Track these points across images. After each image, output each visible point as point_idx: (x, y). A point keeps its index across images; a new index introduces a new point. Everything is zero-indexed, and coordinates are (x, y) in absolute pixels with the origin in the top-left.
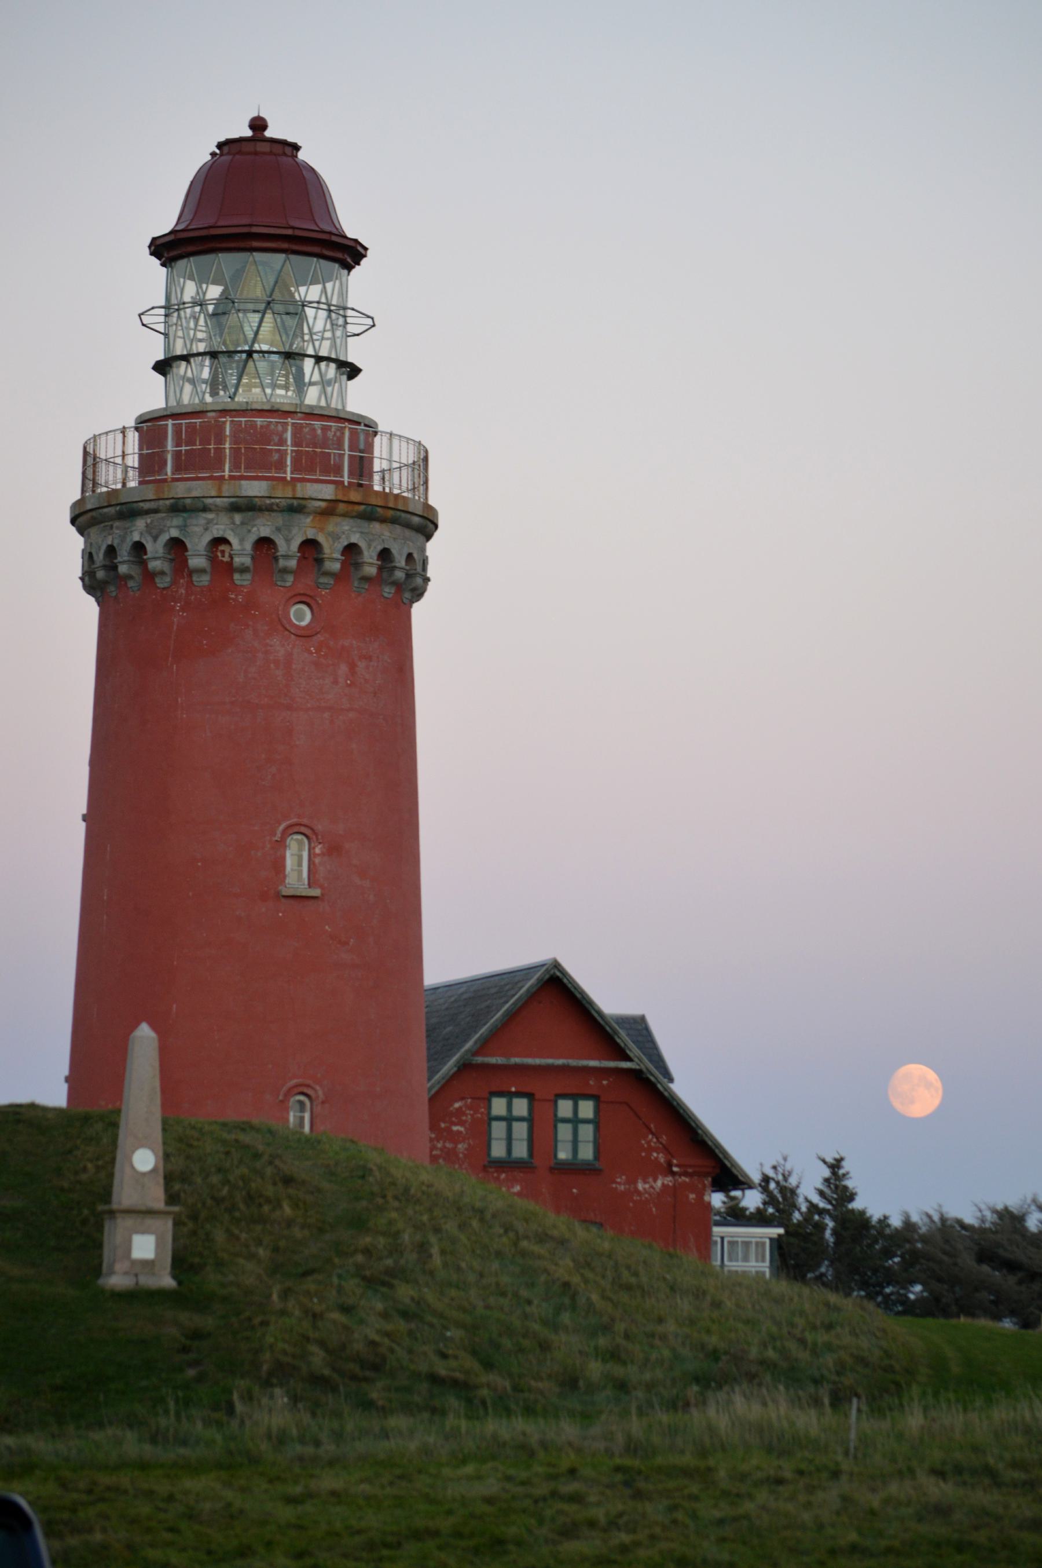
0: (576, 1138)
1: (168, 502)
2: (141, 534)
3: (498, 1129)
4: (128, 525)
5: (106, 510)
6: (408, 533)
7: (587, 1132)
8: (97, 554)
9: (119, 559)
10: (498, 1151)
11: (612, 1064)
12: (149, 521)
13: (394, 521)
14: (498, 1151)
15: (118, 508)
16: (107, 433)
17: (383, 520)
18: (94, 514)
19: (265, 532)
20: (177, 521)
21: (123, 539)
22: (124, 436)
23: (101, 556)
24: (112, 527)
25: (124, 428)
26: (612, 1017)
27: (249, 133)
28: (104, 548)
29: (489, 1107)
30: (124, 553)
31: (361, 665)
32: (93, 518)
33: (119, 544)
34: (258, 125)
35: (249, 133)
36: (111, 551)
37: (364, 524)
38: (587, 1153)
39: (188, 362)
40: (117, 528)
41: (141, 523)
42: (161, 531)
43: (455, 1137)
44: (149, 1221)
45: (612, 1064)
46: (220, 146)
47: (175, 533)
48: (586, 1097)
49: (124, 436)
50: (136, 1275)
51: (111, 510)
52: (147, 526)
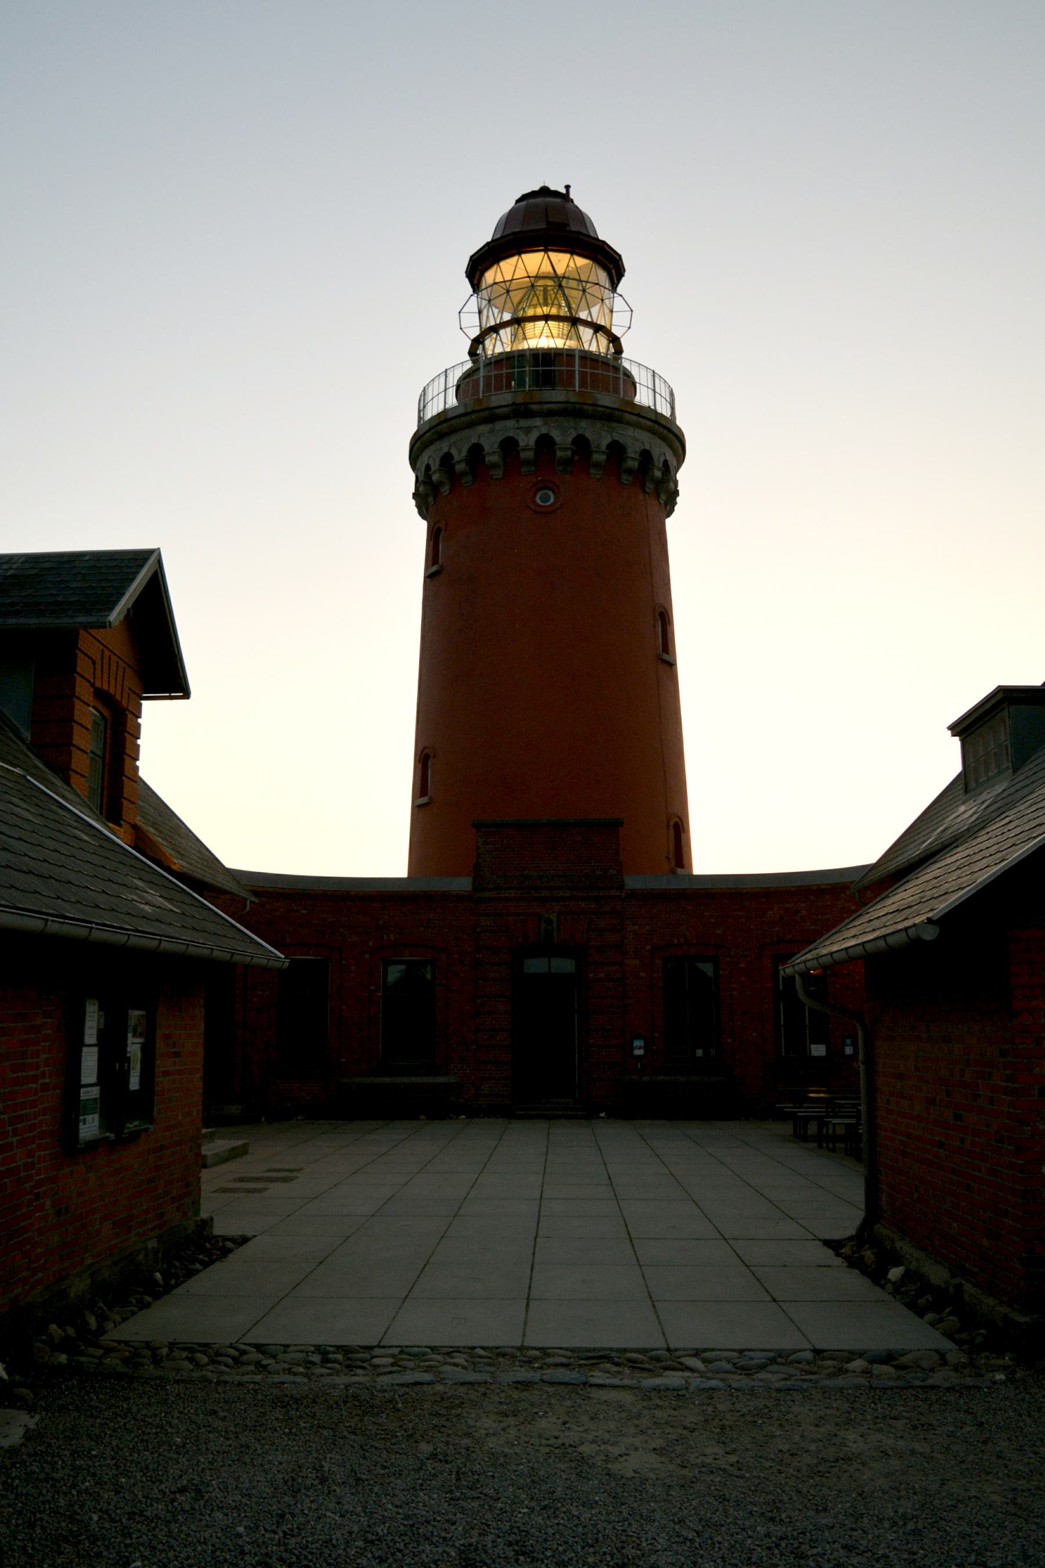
39: (497, 333)
46: (517, 201)
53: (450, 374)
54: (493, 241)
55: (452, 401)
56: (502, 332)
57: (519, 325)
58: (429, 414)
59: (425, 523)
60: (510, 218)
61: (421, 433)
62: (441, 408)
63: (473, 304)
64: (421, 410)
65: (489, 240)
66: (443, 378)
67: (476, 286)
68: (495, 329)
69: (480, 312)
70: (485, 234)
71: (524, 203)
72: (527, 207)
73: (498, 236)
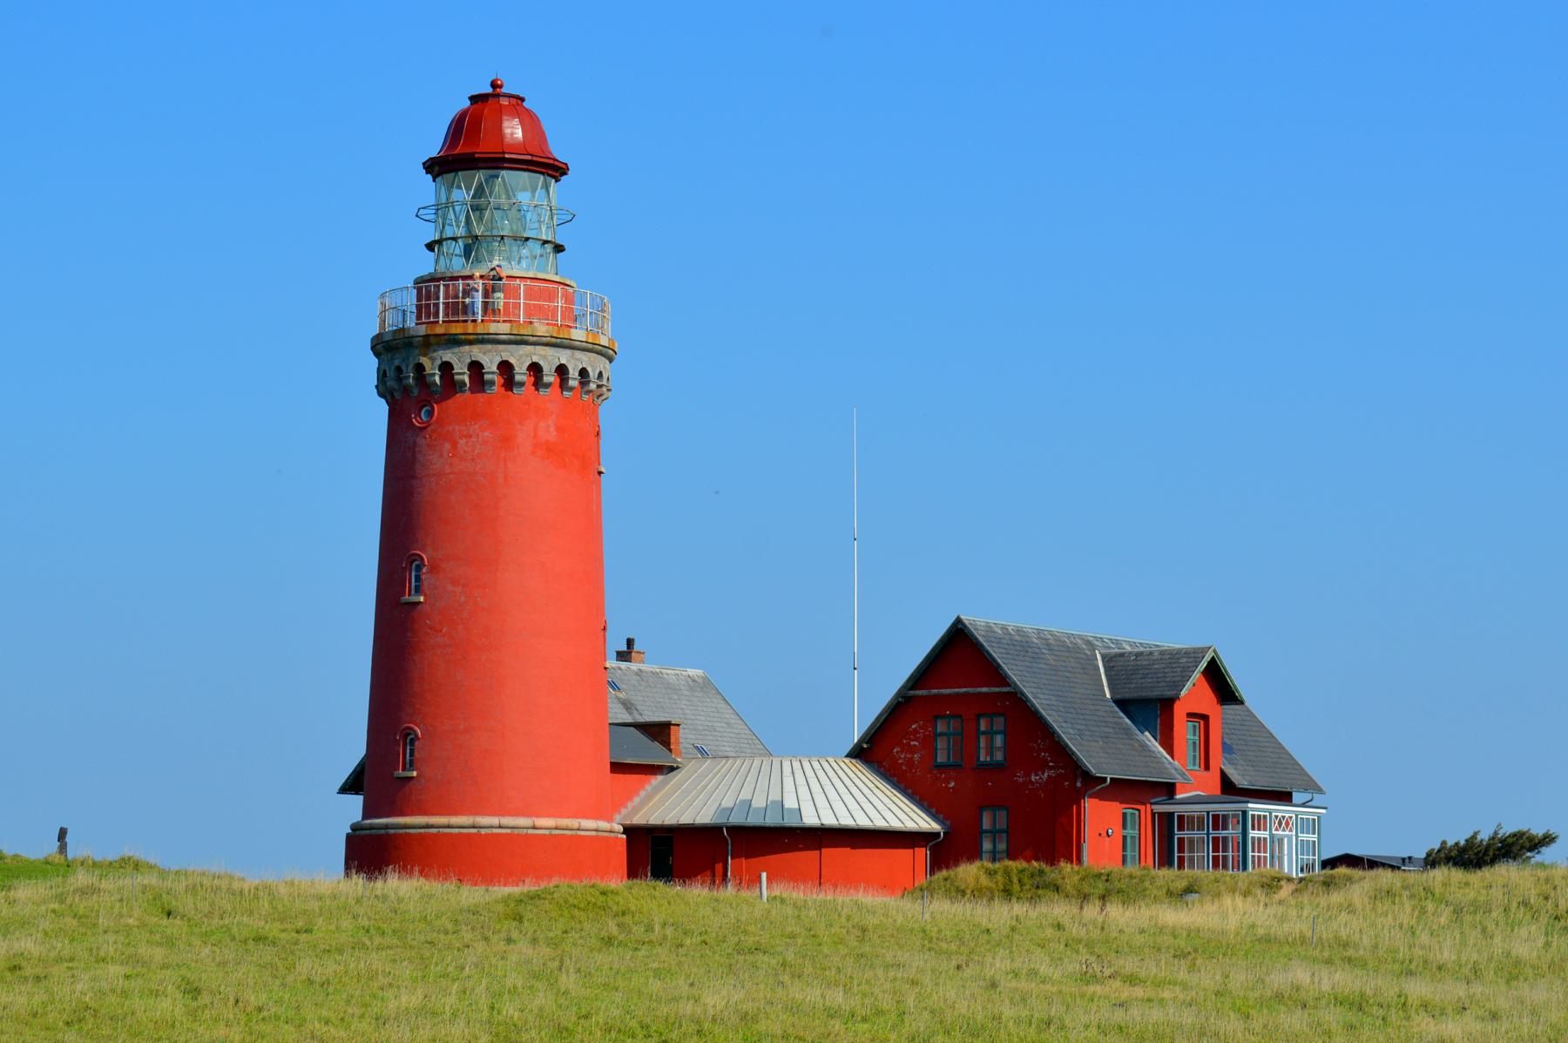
0: (992, 747)
3: (941, 744)
6: (501, 347)
7: (999, 740)
10: (941, 758)
11: (997, 690)
13: (482, 342)
14: (941, 758)
17: (471, 343)
19: (397, 363)
26: (1069, 655)
27: (490, 90)
29: (935, 727)
31: (462, 442)
34: (494, 85)
35: (490, 90)
37: (456, 350)
38: (999, 756)
43: (912, 750)
45: (997, 690)
48: (998, 714)
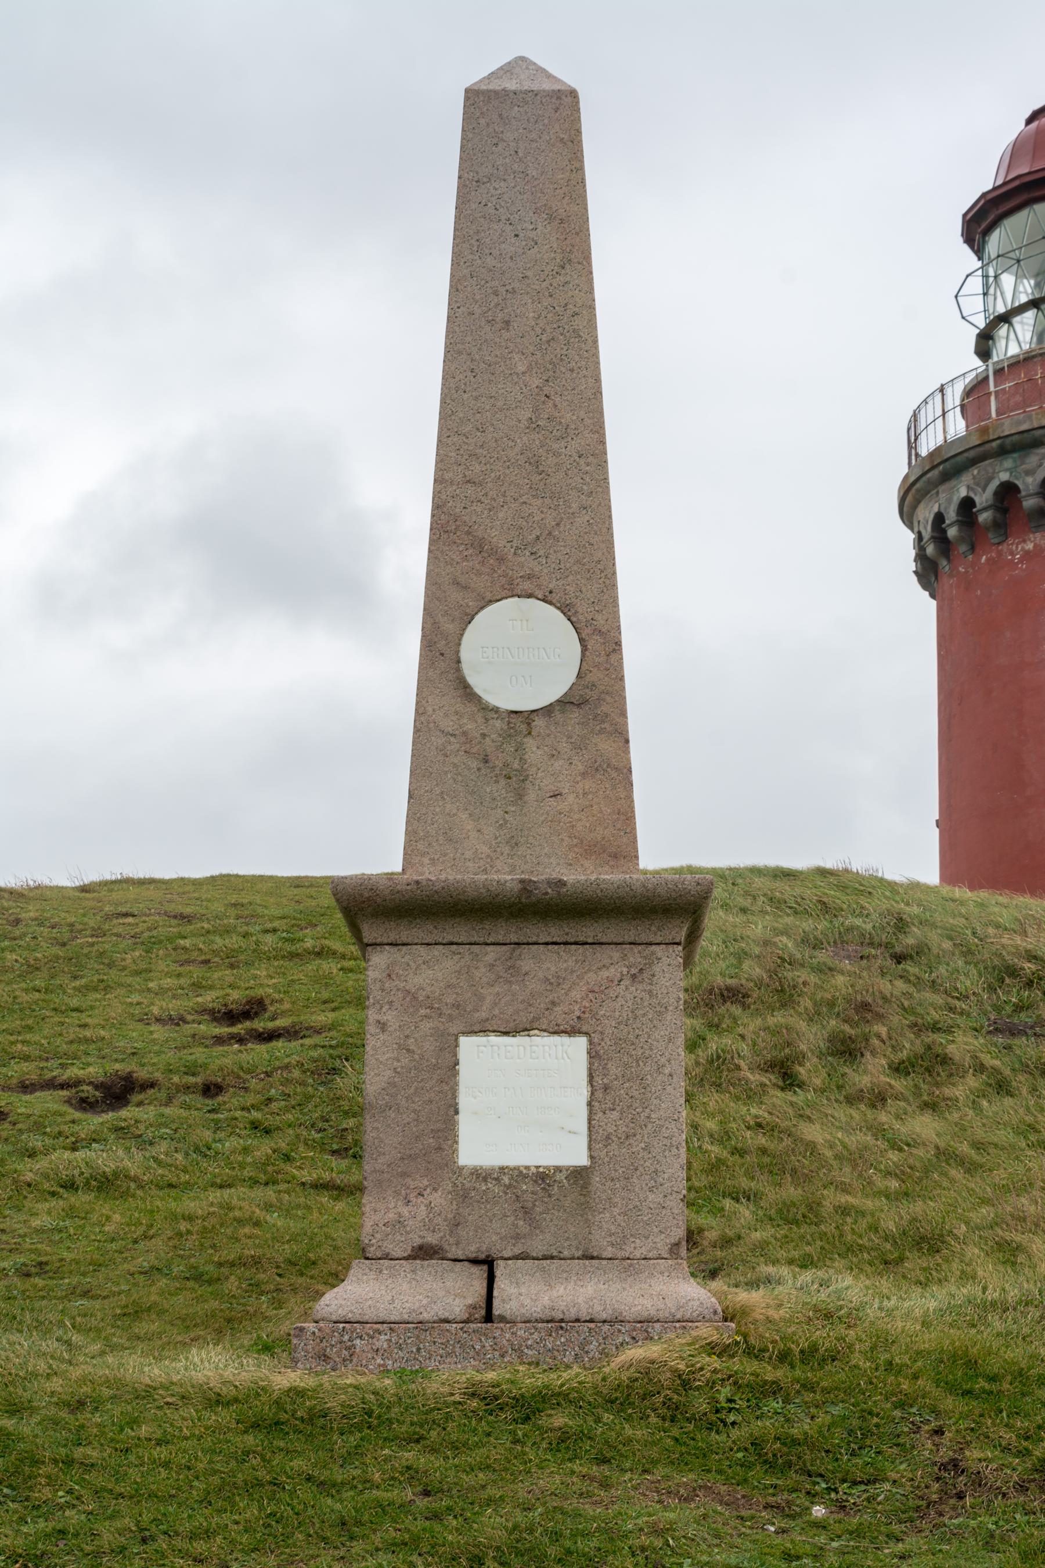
1: (994, 444)
2: (968, 487)
4: (953, 482)
5: (929, 475)
8: (925, 528)
9: (947, 522)
12: (975, 472)
15: (941, 467)
16: (925, 401)
18: (918, 486)
20: (1008, 463)
21: (949, 501)
22: (943, 395)
23: (929, 528)
24: (937, 493)
25: (942, 385)
28: (932, 516)
30: (951, 515)
32: (918, 491)
33: (946, 509)
36: (939, 518)
39: (1010, 324)
40: (943, 492)
41: (967, 478)
42: (989, 480)
44: (547, 965)
46: (1029, 121)
47: (1004, 476)
49: (943, 395)
50: (488, 1263)
51: (935, 473)
52: (974, 477)
53: (948, 391)
54: (995, 189)
55: (957, 426)
56: (1016, 320)
57: (1038, 308)
58: (924, 452)
59: (934, 603)
60: (1016, 150)
61: (912, 479)
62: (940, 441)
63: (976, 284)
64: (912, 446)
65: (990, 187)
66: (938, 397)
67: (979, 252)
68: (1005, 318)
69: (985, 294)
70: (983, 177)
71: (1034, 125)
72: (1038, 131)
73: (999, 182)
